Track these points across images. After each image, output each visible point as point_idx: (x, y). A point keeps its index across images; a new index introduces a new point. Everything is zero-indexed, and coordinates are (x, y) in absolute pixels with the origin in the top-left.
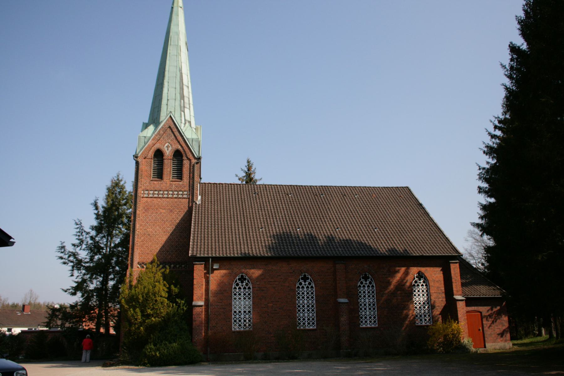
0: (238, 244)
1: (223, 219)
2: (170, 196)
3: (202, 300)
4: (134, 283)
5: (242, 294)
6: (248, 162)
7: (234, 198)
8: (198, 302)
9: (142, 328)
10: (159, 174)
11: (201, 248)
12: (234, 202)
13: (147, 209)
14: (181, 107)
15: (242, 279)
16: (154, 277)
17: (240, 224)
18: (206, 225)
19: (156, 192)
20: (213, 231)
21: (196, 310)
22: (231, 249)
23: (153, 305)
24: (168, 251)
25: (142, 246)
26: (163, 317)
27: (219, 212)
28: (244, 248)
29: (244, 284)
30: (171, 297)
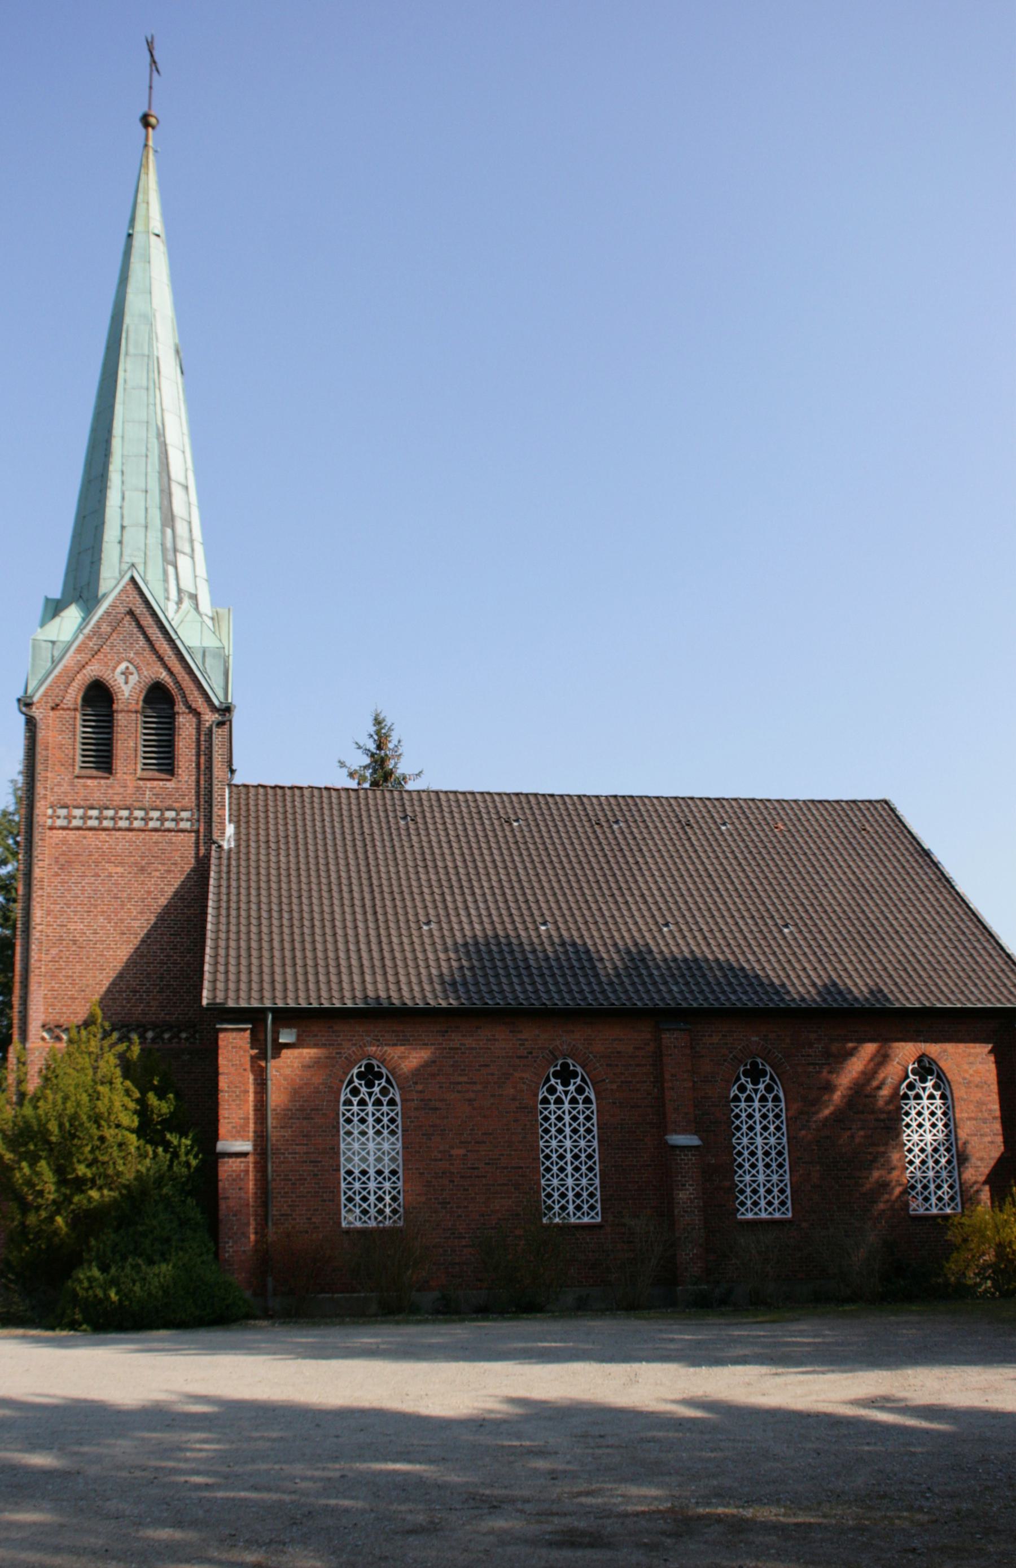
0: (356, 970)
1: (305, 894)
2: (137, 824)
3: (244, 1138)
4: (32, 1085)
5: (370, 1120)
6: (378, 722)
7: (338, 831)
8: (236, 1141)
9: (59, 1219)
10: (102, 758)
11: (238, 981)
12: (339, 842)
13: (65, 864)
14: (164, 550)
15: (369, 1076)
16: (95, 1069)
17: (358, 910)
18: (254, 914)
19: (94, 813)
20: (275, 930)
21: (227, 1168)
22: (334, 987)
23: (92, 1151)
24: (135, 992)
25: (53, 976)
26: (126, 1187)
27: (293, 873)
28: (375, 982)
29: (376, 1089)
30: (148, 1129)
